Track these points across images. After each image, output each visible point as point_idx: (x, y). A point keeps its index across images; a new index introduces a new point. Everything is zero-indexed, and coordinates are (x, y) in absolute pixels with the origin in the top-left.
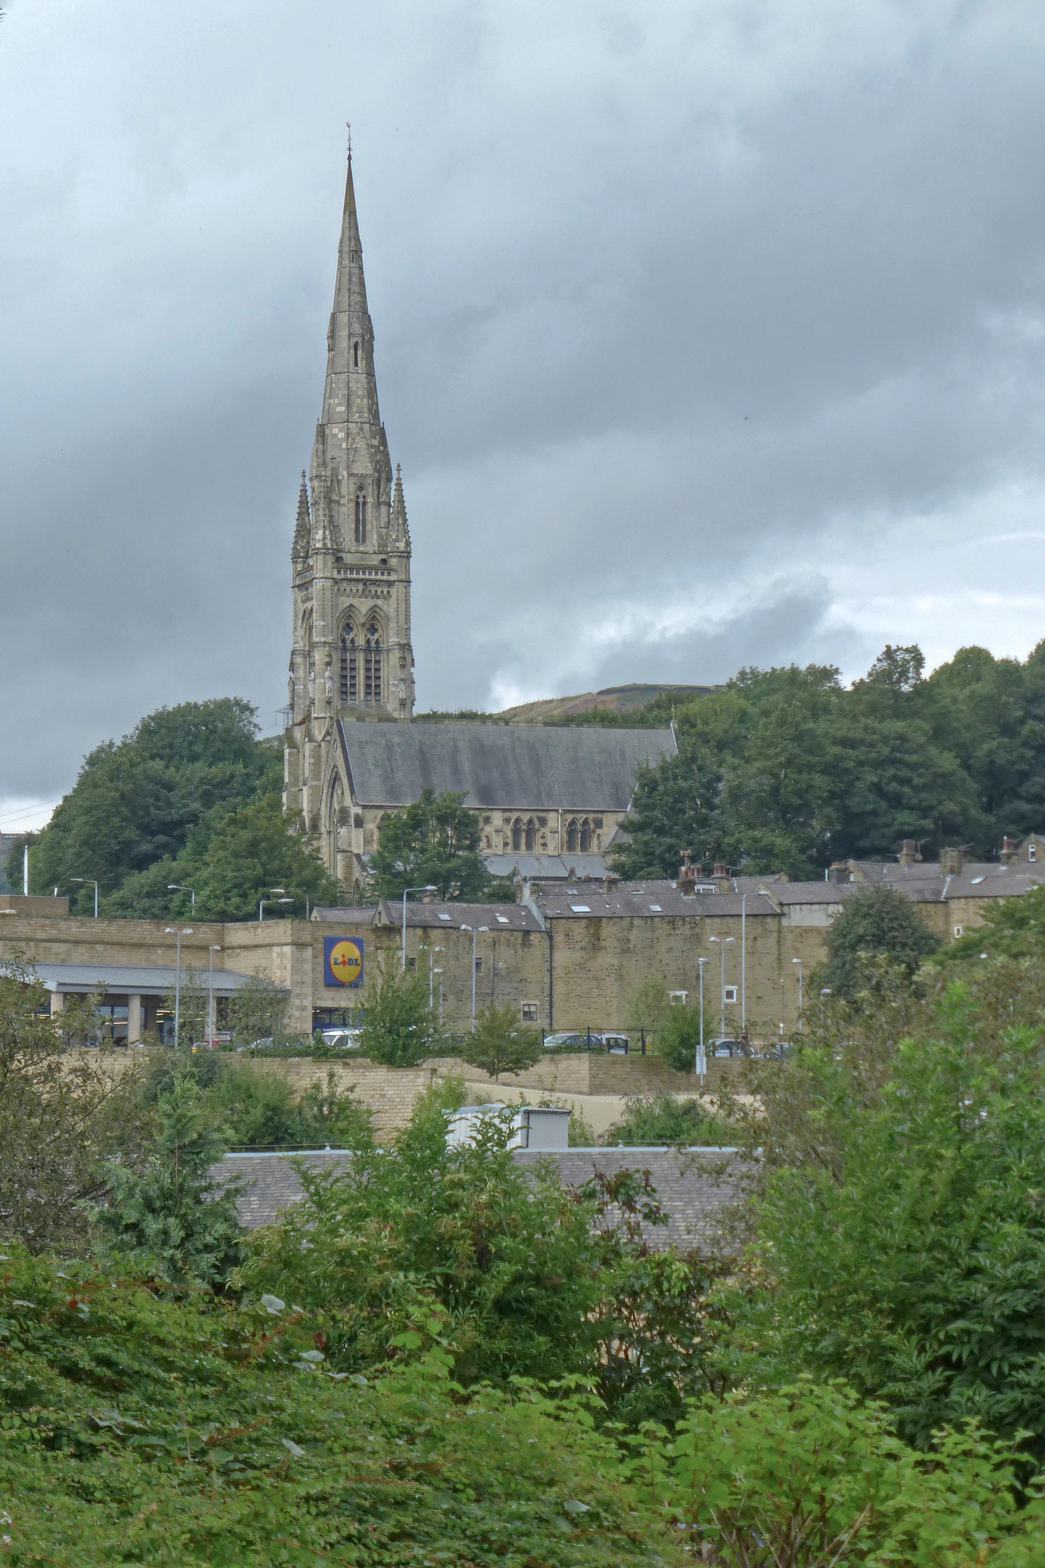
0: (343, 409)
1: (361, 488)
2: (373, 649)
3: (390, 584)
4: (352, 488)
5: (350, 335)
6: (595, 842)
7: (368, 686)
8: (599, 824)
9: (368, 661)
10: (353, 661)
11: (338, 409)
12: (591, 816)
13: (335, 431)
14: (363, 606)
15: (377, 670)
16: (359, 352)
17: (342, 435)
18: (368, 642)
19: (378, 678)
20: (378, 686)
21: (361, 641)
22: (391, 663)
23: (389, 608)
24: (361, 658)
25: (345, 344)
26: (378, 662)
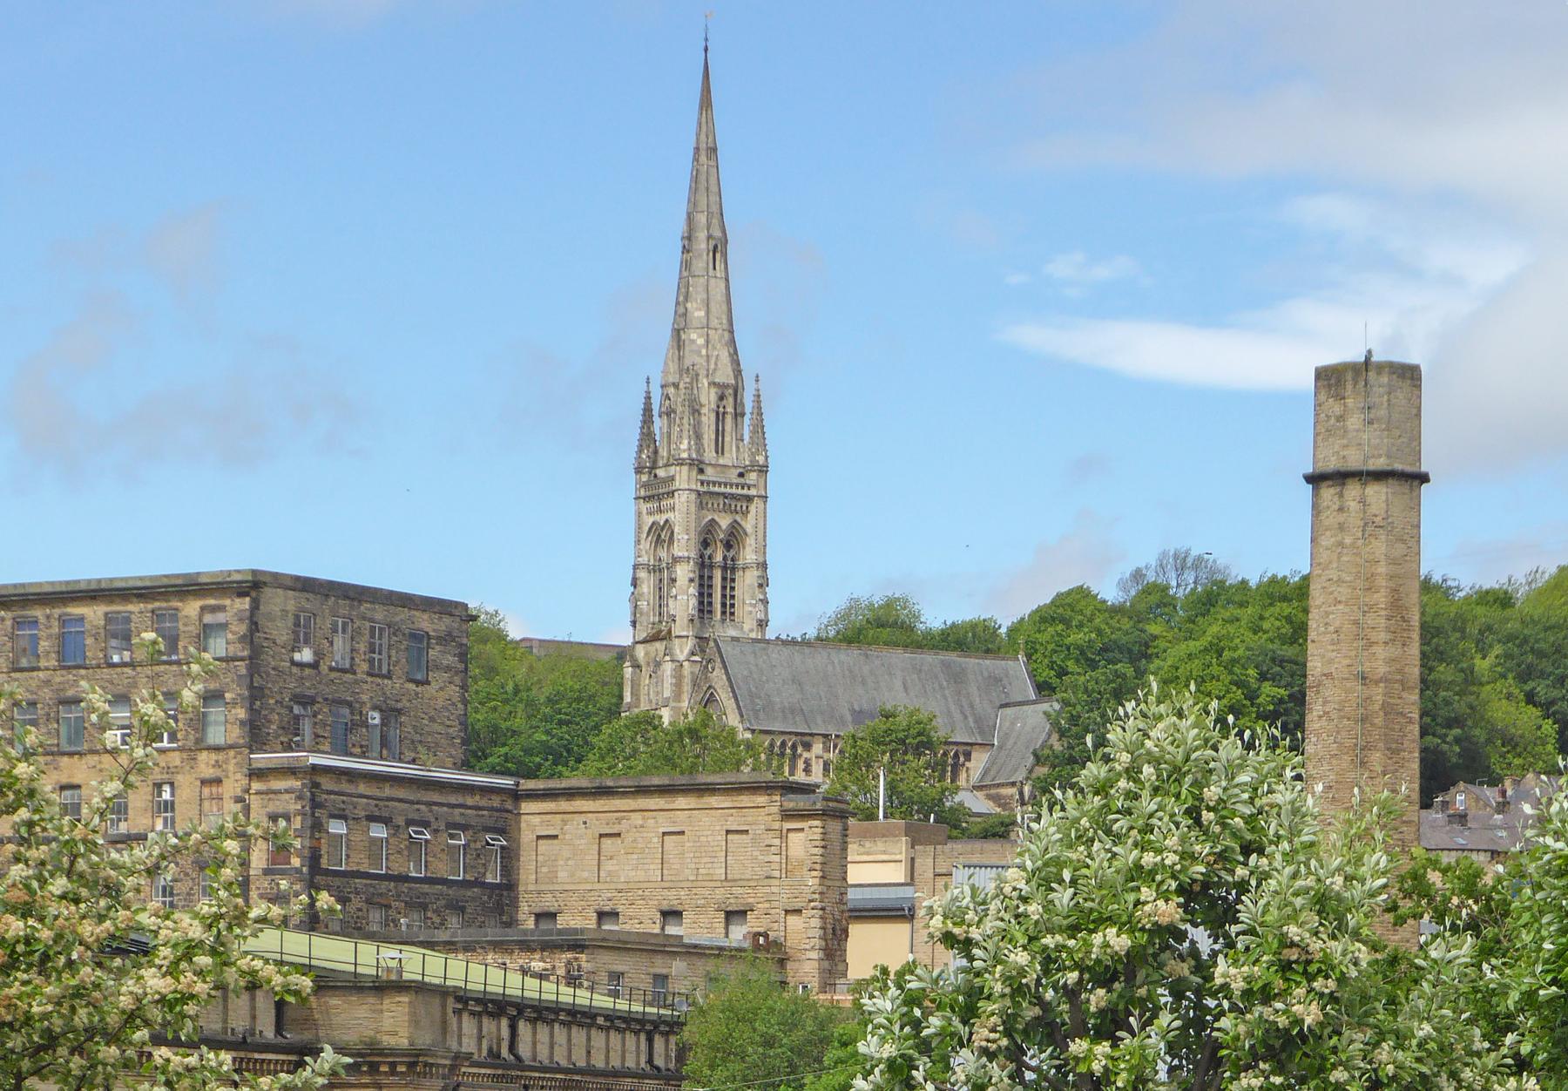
0: (702, 313)
1: (721, 398)
2: (730, 568)
3: (749, 499)
4: (713, 397)
5: (709, 237)
6: (963, 775)
7: (724, 605)
8: (968, 756)
9: (724, 579)
10: (710, 578)
11: (696, 314)
12: (961, 748)
13: (694, 336)
14: (724, 522)
15: (733, 589)
16: (718, 256)
17: (701, 341)
18: (725, 558)
19: (733, 597)
20: (732, 606)
21: (719, 558)
22: (748, 581)
23: (748, 525)
24: (718, 574)
25: (703, 246)
26: (733, 580)
